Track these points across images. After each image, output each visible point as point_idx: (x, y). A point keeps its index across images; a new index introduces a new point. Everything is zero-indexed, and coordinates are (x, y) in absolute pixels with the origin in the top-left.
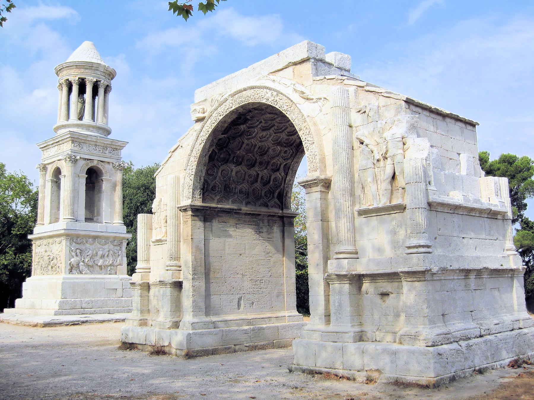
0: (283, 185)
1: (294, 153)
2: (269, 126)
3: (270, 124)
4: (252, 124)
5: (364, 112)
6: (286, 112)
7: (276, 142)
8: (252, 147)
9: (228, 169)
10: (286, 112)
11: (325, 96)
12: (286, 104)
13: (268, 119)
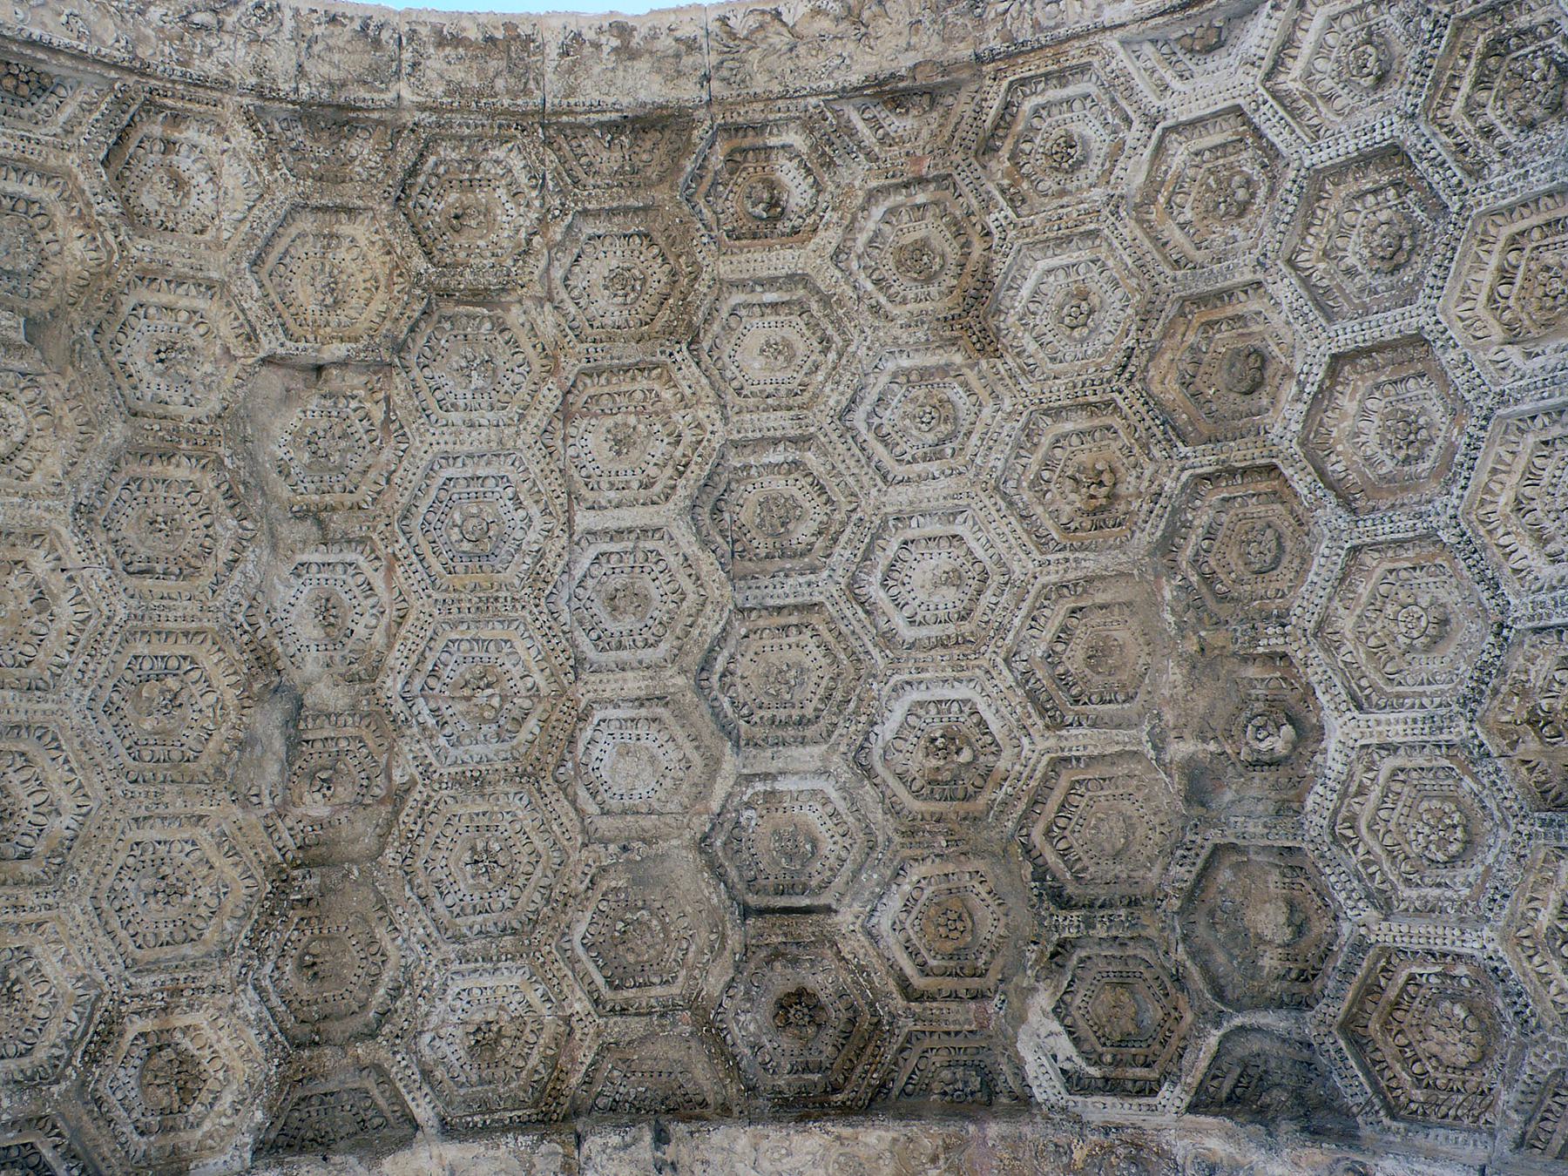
4: (834, 814)
7: (971, 376)
9: (1375, 793)
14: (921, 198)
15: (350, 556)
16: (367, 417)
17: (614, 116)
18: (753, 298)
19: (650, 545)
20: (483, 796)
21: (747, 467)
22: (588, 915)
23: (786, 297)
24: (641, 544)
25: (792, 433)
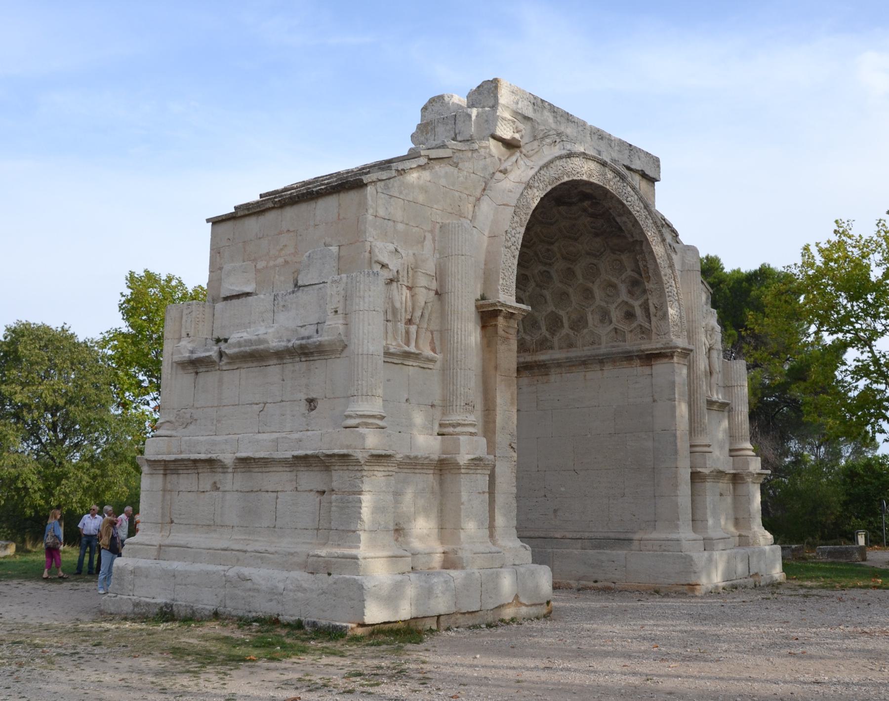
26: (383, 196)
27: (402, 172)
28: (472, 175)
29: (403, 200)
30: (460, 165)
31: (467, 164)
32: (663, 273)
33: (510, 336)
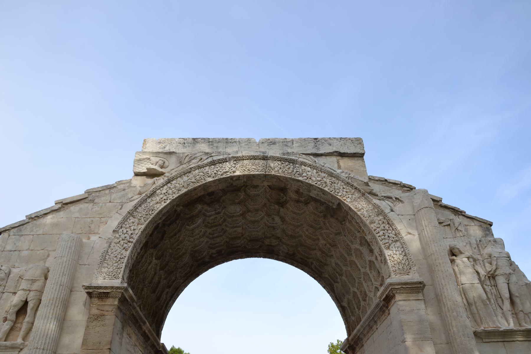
0: (163, 308)
1: (190, 272)
2: (212, 223)
3: (214, 223)
5: (447, 225)
6: (344, 198)
8: (175, 243)
10: (344, 198)
11: (398, 197)
12: (345, 190)
13: (227, 213)
14: (199, 257)
15: (270, 224)
16: (267, 232)
17: (236, 254)
18: (219, 244)
19: (232, 226)
20: (255, 208)
21: (219, 233)
22: (241, 198)
23: (215, 245)
24: (233, 225)
25: (215, 239)
26: (14, 237)
27: (35, 218)
28: (108, 204)
29: (33, 235)
30: (95, 201)
31: (103, 199)
32: (368, 222)
33: (106, 313)
